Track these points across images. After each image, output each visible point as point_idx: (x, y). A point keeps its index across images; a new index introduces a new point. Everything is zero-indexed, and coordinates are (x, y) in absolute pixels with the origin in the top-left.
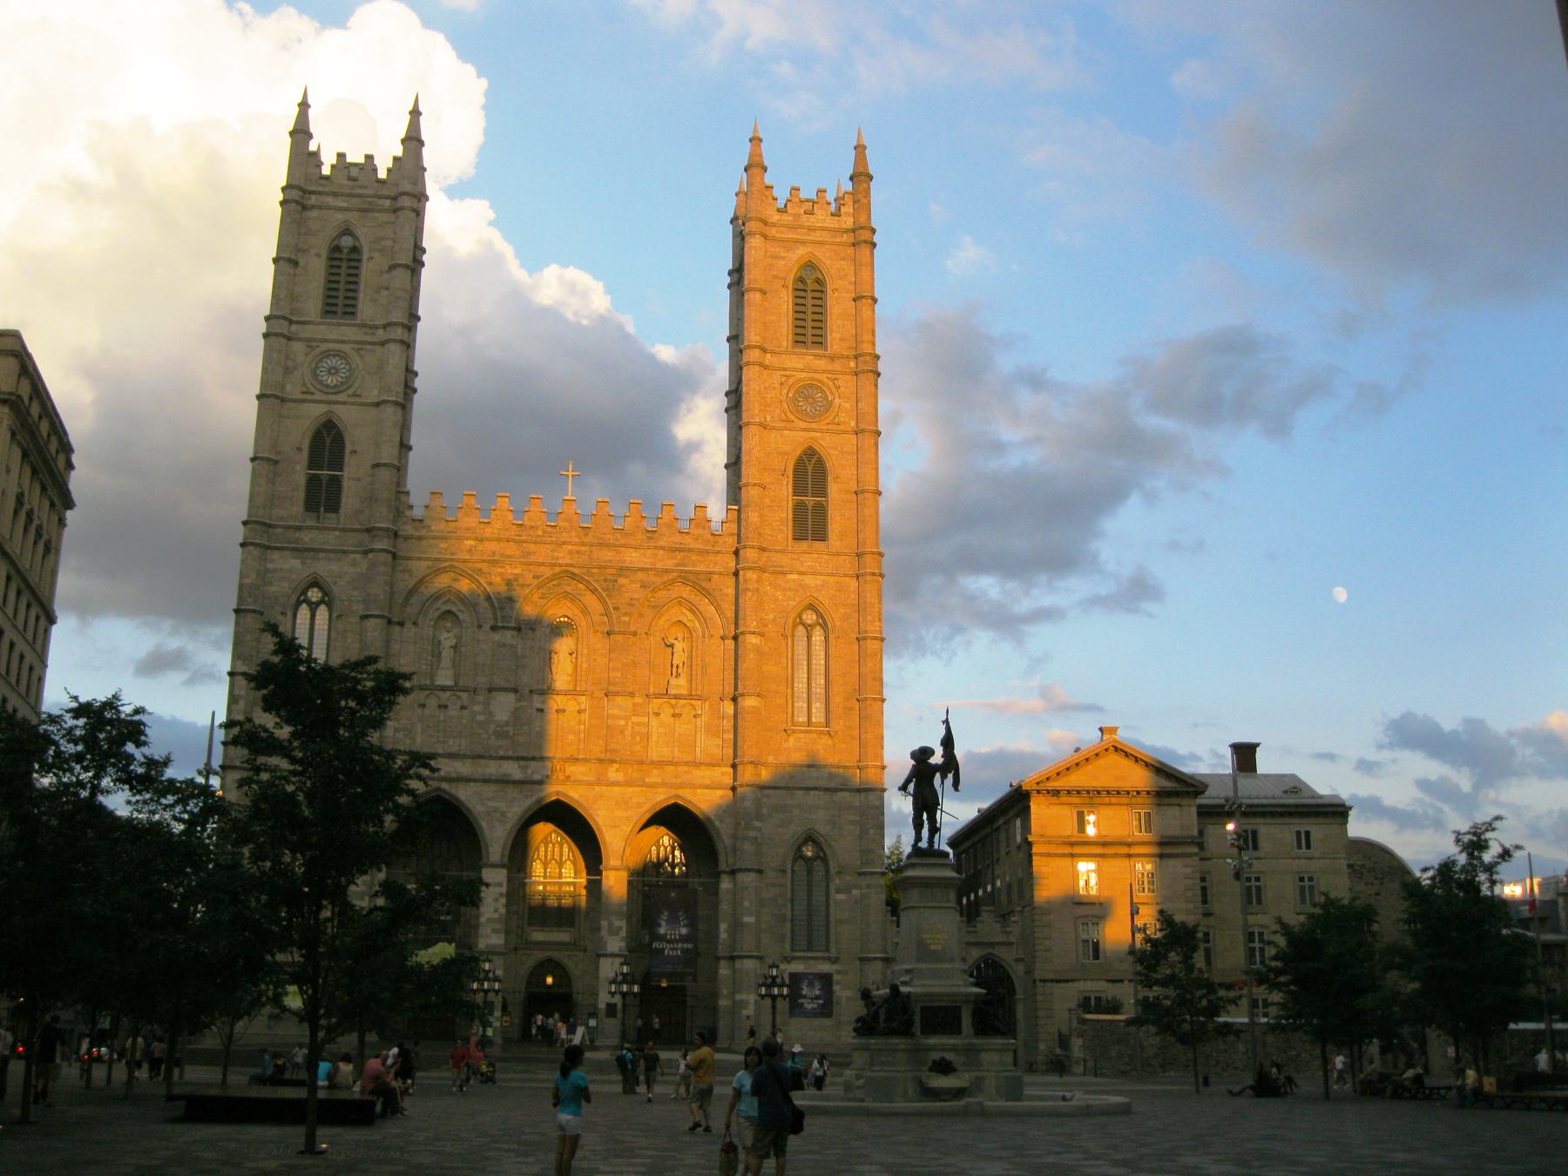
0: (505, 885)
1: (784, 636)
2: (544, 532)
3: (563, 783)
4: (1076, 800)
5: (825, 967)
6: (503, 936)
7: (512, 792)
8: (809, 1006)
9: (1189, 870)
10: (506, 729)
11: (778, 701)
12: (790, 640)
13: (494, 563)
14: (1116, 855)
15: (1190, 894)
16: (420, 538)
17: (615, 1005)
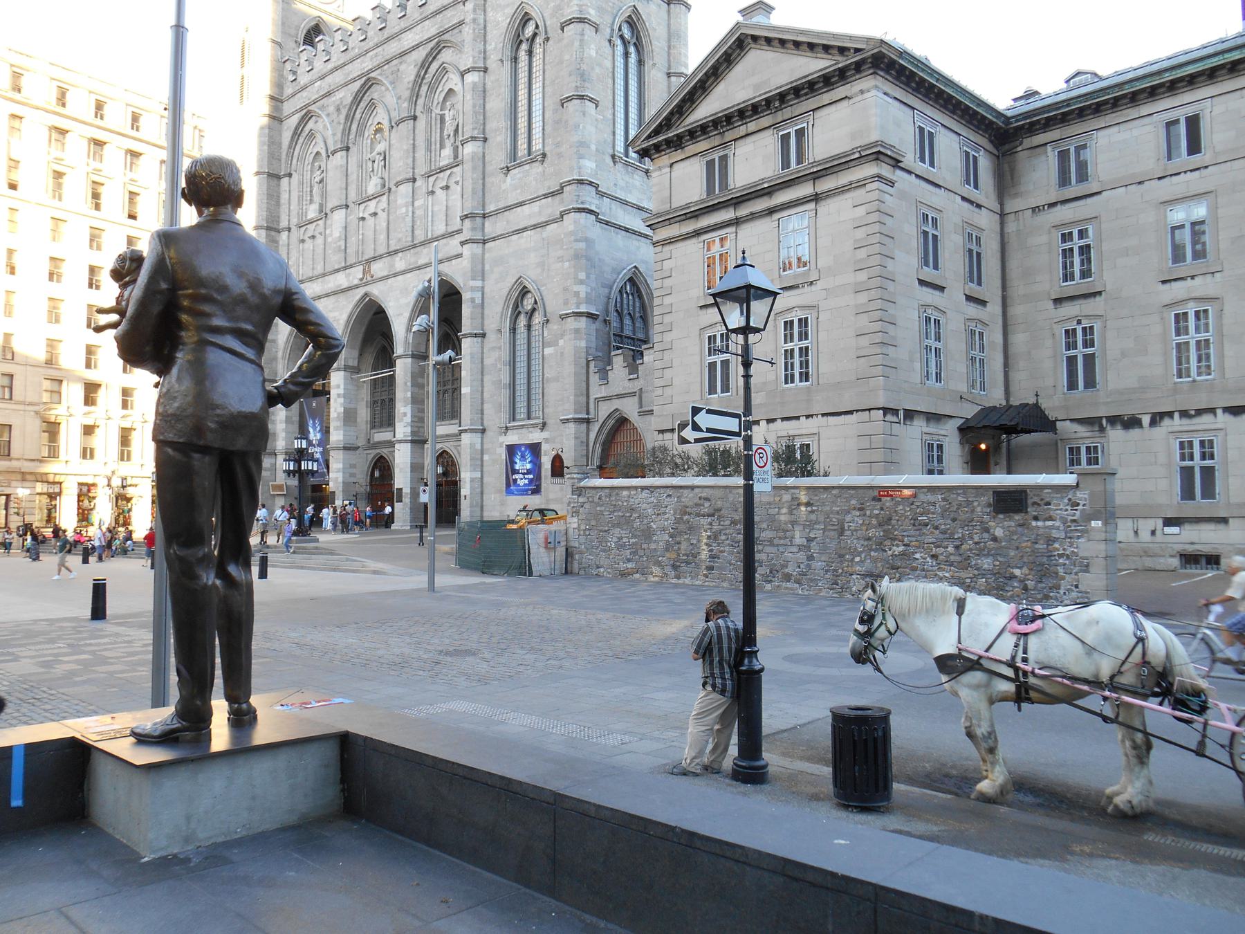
0: (342, 387)
1: (502, 61)
2: (359, 48)
3: (367, 284)
4: (703, 145)
5: (535, 436)
6: (342, 432)
7: (342, 298)
8: (521, 483)
9: (861, 211)
10: (338, 244)
11: (499, 139)
12: (508, 64)
13: (328, 94)
14: (753, 217)
15: (862, 253)
16: (293, 95)
17: (401, 489)
